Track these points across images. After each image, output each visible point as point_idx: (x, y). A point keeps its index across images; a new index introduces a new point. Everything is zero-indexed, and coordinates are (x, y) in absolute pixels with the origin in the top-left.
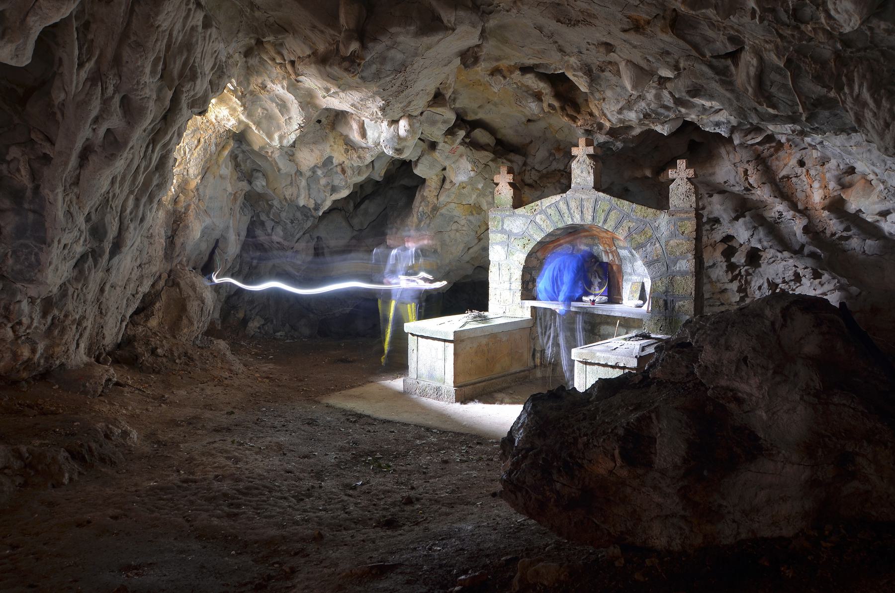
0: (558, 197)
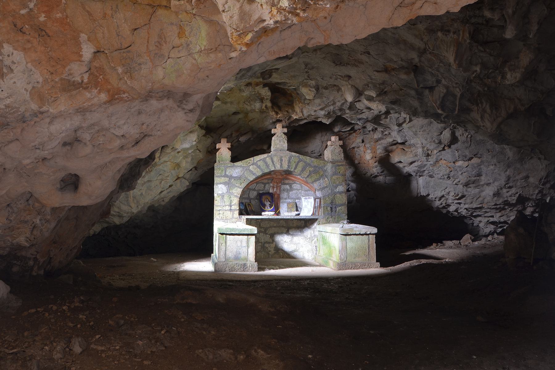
0: (265, 156)
